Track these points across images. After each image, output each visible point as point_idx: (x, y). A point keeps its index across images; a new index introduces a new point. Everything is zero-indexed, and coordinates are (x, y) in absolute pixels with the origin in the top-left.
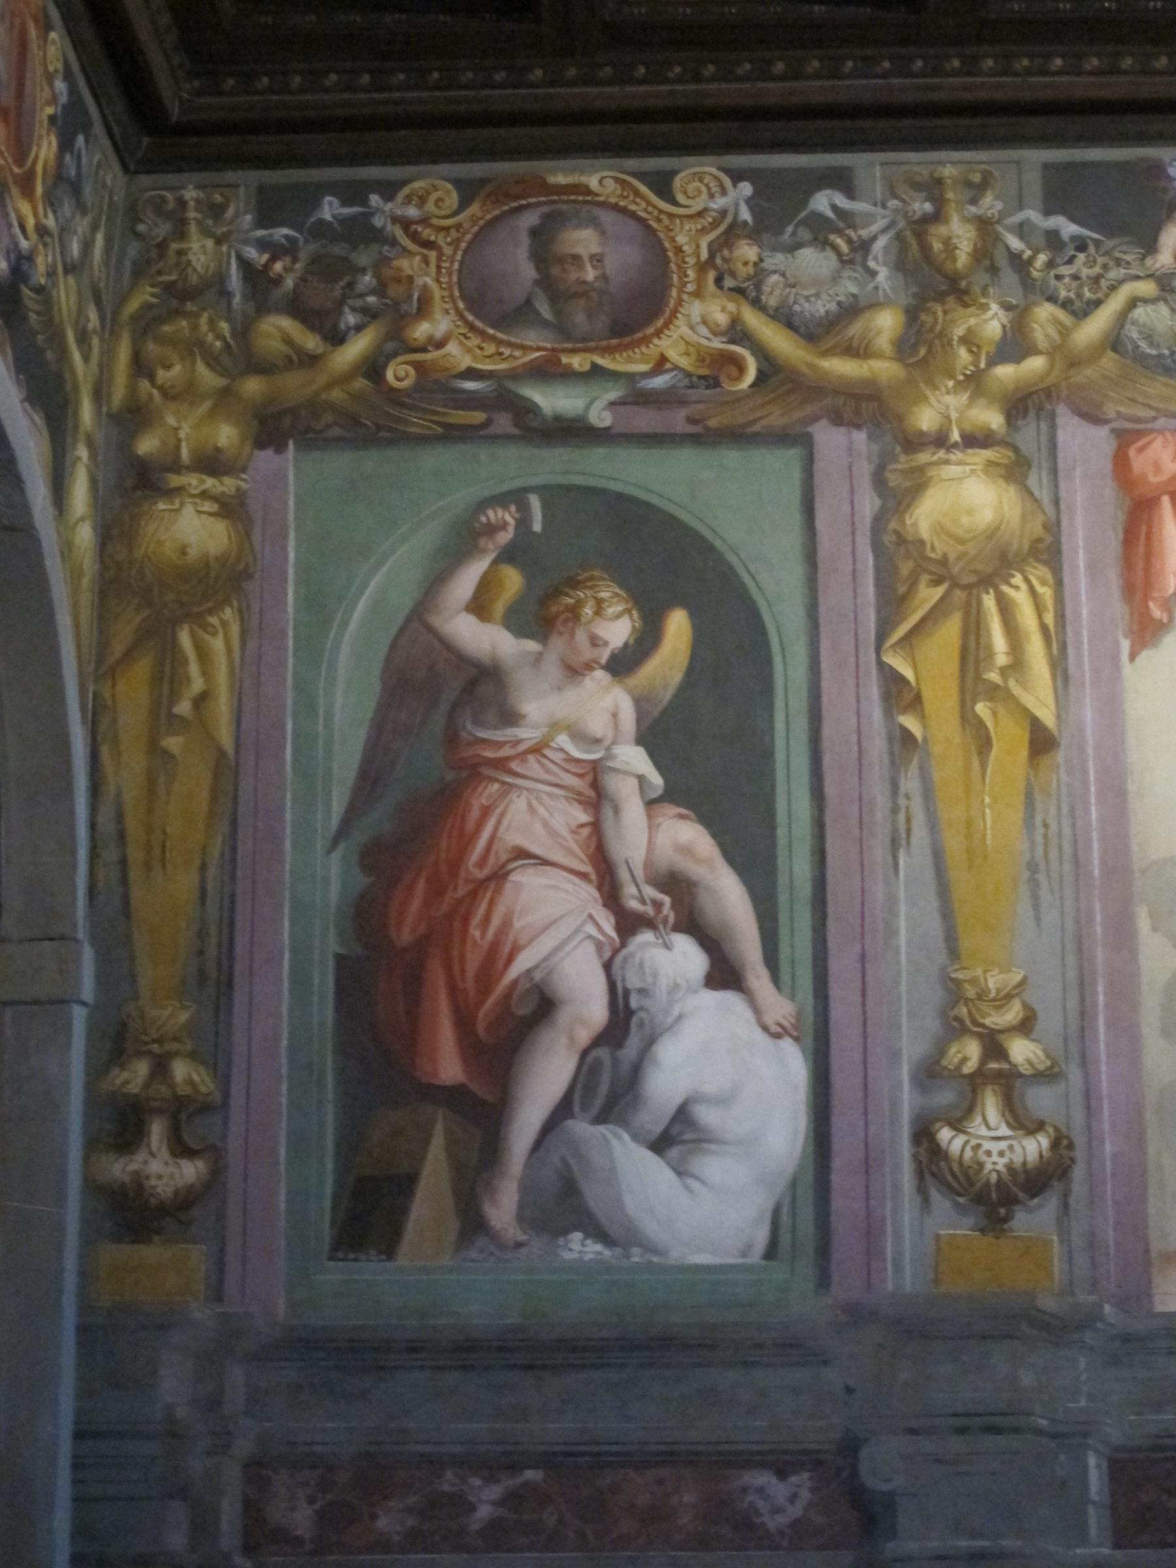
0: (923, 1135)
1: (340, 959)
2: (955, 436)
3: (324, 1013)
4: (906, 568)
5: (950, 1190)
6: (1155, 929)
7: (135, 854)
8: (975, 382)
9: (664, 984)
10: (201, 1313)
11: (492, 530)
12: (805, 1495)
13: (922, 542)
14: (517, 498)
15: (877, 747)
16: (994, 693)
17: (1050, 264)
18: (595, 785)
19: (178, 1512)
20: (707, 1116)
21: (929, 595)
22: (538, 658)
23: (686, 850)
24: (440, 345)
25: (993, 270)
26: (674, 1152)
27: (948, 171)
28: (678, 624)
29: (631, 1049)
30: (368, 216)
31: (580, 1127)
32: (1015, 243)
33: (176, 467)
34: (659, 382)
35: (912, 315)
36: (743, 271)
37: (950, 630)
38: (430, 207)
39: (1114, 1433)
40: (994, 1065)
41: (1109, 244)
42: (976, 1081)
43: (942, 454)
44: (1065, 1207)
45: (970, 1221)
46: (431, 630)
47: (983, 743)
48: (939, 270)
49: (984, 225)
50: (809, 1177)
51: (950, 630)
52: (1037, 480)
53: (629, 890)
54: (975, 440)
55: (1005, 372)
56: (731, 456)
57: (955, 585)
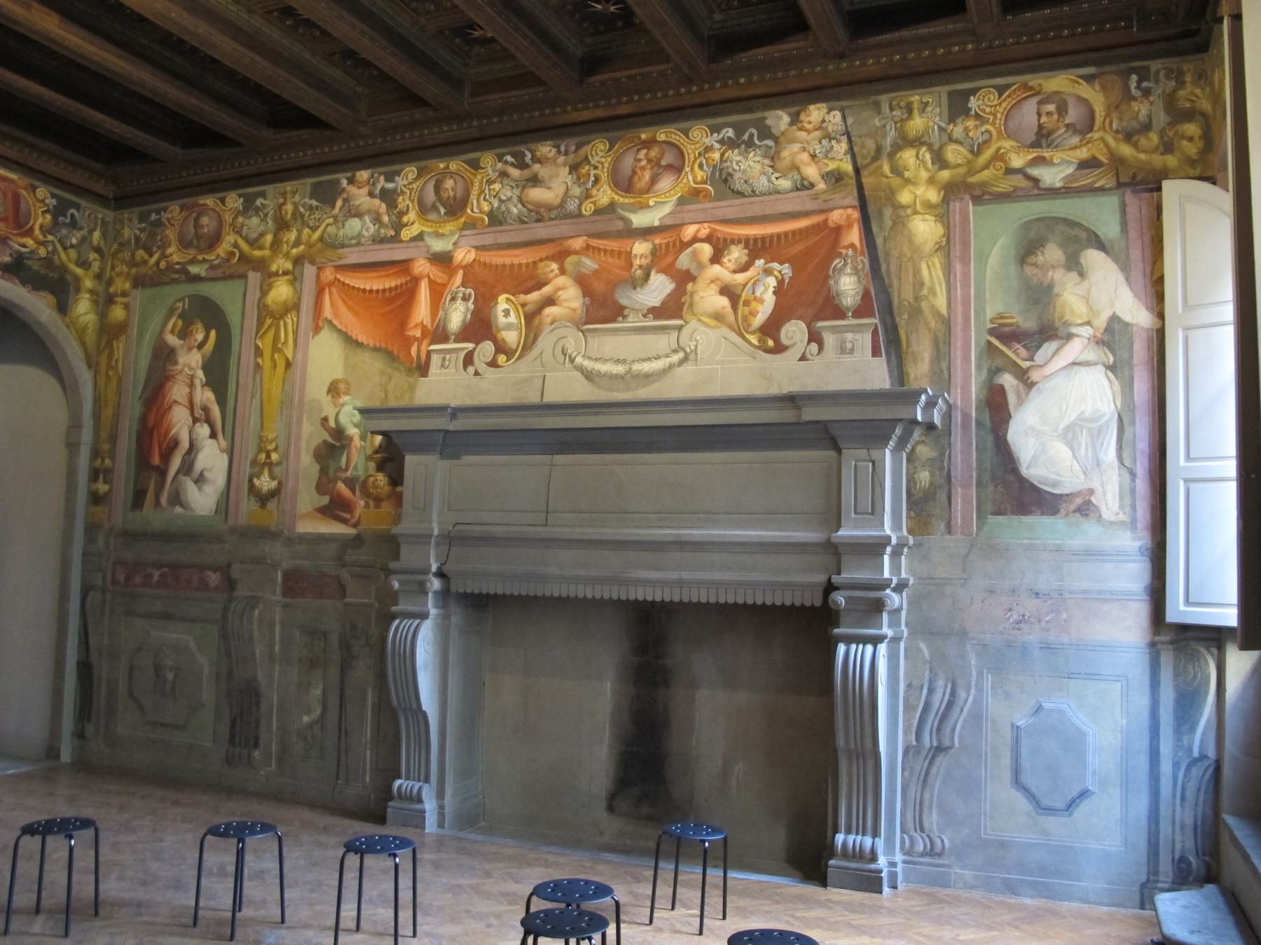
0: (250, 480)
1: (137, 431)
2: (281, 272)
3: (134, 447)
6: (307, 420)
7: (102, 404)
8: (287, 255)
9: (200, 439)
11: (178, 308)
12: (219, 578)
13: (268, 306)
14: (182, 299)
15: (251, 367)
16: (280, 351)
17: (309, 215)
19: (100, 574)
20: (207, 474)
21: (269, 321)
22: (183, 346)
23: (208, 399)
24: (171, 255)
25: (295, 219)
26: (199, 484)
27: (288, 188)
28: (213, 333)
30: (160, 218)
31: (181, 477)
32: (302, 209)
33: (116, 295)
34: (216, 262)
35: (275, 235)
36: (239, 225)
37: (272, 332)
38: (174, 214)
39: (285, 565)
40: (268, 461)
41: (324, 207)
42: (264, 464)
43: (277, 278)
44: (279, 501)
45: (258, 504)
47: (275, 366)
48: (283, 220)
49: (295, 205)
50: (225, 492)
53: (196, 411)
54: (285, 273)
55: (294, 251)
56: (229, 283)
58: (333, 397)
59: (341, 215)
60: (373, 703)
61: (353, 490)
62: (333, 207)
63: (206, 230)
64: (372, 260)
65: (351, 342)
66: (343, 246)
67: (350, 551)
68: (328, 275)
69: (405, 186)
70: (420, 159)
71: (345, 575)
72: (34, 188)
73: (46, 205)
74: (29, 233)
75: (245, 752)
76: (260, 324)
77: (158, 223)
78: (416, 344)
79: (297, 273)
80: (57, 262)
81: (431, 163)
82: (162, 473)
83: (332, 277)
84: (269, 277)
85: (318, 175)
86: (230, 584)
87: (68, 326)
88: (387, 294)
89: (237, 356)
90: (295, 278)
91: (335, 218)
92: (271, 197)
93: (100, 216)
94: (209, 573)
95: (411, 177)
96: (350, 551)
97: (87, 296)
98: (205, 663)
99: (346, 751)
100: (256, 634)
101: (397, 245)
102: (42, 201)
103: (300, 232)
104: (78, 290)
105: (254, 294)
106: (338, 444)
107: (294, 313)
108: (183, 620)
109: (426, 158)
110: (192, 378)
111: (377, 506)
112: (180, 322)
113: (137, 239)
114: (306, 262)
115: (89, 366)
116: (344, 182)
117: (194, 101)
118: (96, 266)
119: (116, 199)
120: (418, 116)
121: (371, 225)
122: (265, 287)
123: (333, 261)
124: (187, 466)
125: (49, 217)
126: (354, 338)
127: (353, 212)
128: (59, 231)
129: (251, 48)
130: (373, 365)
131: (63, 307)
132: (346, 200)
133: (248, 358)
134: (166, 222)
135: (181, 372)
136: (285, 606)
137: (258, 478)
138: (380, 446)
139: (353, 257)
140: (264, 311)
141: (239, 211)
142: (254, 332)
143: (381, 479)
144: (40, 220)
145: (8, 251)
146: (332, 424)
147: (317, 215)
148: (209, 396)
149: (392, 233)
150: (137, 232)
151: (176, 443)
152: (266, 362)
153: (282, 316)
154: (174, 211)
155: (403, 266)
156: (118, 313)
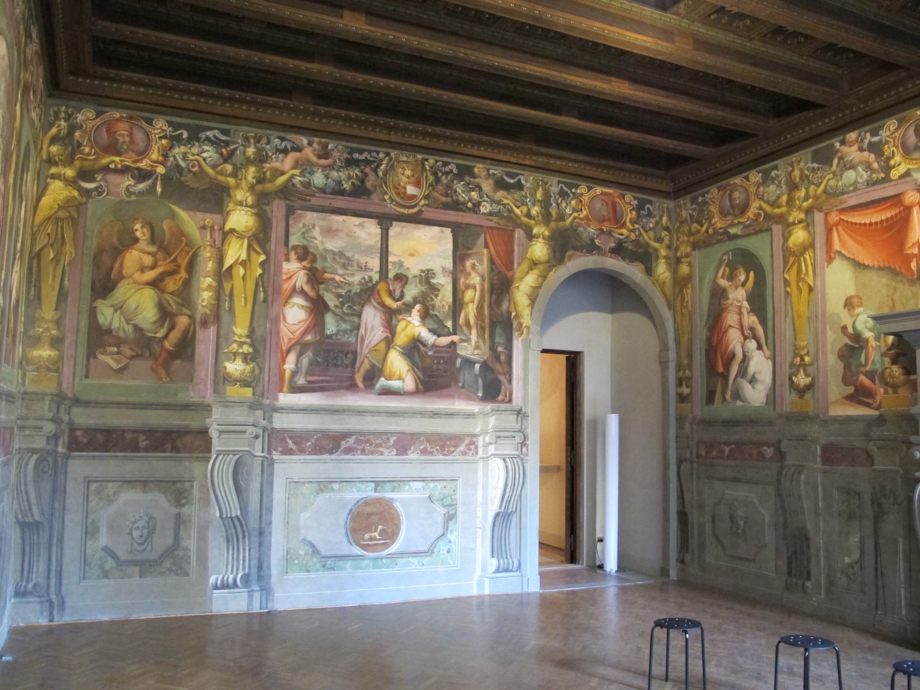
0: (790, 378)
1: (706, 350)
3: (704, 360)
4: (788, 255)
5: (794, 390)
6: (830, 329)
8: (800, 208)
10: (690, 415)
11: (725, 260)
14: (727, 253)
15: (783, 296)
16: (804, 280)
18: (740, 310)
19: (689, 451)
20: (757, 376)
21: (792, 259)
22: (731, 285)
23: (754, 322)
24: (716, 223)
25: (803, 180)
28: (752, 274)
29: (746, 364)
31: (739, 379)
32: (807, 172)
33: (682, 258)
34: (748, 222)
36: (761, 193)
37: (795, 268)
39: (823, 441)
42: (800, 366)
46: (716, 283)
47: (800, 292)
49: (801, 170)
51: (795, 268)
52: (811, 228)
54: (800, 222)
55: (805, 204)
56: (760, 236)
57: (796, 256)
58: (849, 310)
59: (838, 170)
60: (904, 552)
61: (873, 380)
62: (831, 166)
63: (738, 201)
64: (868, 200)
65: (858, 266)
66: (843, 193)
67: (874, 429)
68: (834, 217)
69: (888, 136)
70: (899, 112)
71: (872, 447)
72: (623, 196)
73: (632, 205)
74: (624, 225)
75: (800, 582)
76: (786, 261)
77: (705, 203)
78: (915, 260)
79: (809, 220)
80: (643, 241)
81: (908, 113)
82: (725, 377)
83: (837, 218)
84: (788, 227)
85: (816, 144)
86: (781, 456)
87: (653, 283)
88: (885, 224)
89: (771, 289)
90: (808, 224)
91: (834, 173)
92: (781, 168)
93: (665, 206)
94: (765, 448)
95: (892, 128)
96: (874, 429)
97: (663, 261)
98: (766, 515)
99: (883, 587)
100: (803, 493)
101: (887, 185)
102: (629, 203)
103: (807, 189)
104: (657, 258)
105: (778, 242)
106: (857, 346)
107: (811, 250)
108: (748, 482)
109: (904, 110)
110: (740, 308)
111: (895, 392)
112: (727, 270)
113: (691, 216)
114: (815, 211)
115: (670, 308)
116: (837, 145)
117: (719, 113)
118: (667, 239)
119: (674, 192)
120: (892, 79)
121: (864, 173)
122: (786, 235)
123: (836, 206)
124: (743, 372)
125: (634, 213)
126: (861, 261)
127: (848, 166)
128: (642, 221)
129: (755, 65)
130: (879, 282)
131: (649, 271)
132: (841, 158)
133: (779, 288)
134: (709, 201)
135: (732, 304)
136: (825, 472)
137: (796, 376)
138: (893, 344)
139: (852, 200)
140: (787, 252)
141: (760, 183)
142: (782, 269)
143: (896, 370)
144: (629, 216)
145: (613, 240)
146: (850, 330)
147: (819, 175)
148: (751, 320)
149: (883, 175)
150: (691, 212)
151: (733, 355)
152: (793, 289)
153: (802, 254)
154: (714, 192)
155: (896, 199)
156: (684, 269)
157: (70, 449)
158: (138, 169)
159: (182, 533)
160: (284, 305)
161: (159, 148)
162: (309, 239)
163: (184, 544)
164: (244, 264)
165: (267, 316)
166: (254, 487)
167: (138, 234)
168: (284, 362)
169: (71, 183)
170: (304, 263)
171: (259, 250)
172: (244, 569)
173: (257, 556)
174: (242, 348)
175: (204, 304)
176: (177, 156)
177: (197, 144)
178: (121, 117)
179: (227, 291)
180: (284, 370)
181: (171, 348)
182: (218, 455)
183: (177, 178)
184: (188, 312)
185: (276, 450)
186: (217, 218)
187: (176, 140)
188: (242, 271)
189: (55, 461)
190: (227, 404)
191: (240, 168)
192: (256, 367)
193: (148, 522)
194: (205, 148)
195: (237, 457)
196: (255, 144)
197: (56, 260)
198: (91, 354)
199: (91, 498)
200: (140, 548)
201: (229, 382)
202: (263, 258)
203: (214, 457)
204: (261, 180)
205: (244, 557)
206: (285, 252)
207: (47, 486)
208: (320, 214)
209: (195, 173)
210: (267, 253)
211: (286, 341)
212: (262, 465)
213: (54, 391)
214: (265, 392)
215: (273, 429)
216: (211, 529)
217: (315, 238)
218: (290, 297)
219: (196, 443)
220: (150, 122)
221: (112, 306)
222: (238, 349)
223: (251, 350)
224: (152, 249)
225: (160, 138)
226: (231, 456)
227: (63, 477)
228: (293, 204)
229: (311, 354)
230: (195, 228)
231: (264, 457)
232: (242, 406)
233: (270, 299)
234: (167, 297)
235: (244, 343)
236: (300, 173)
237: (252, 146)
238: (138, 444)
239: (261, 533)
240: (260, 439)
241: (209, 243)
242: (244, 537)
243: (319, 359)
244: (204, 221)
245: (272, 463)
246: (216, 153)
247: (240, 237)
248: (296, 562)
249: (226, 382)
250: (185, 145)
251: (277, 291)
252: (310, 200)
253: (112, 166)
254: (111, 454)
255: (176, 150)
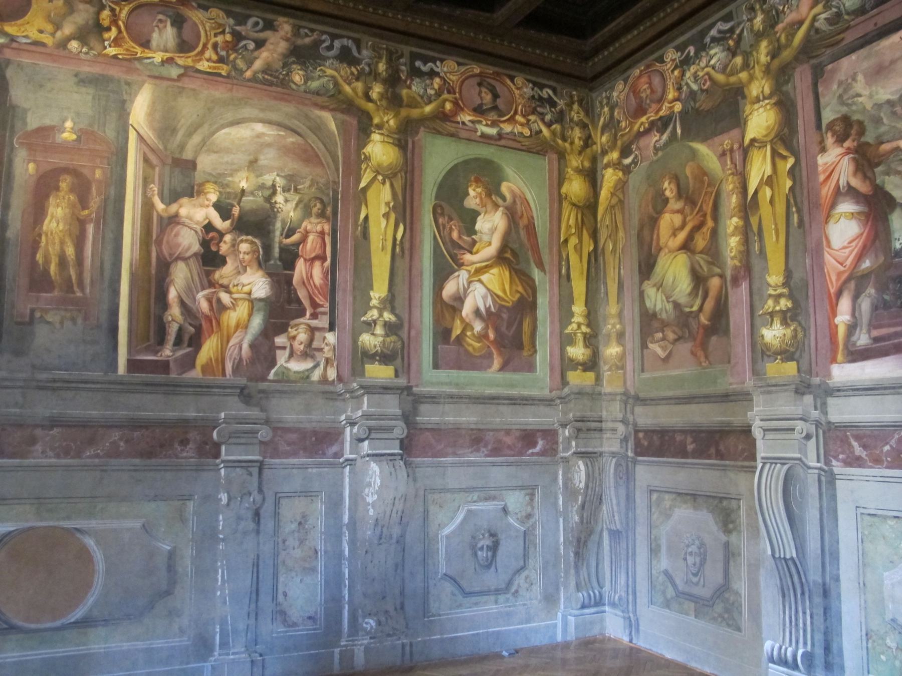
157: (637, 454)
158: (661, 118)
159: (732, 570)
160: (827, 222)
161: (673, 84)
162: (850, 101)
163: (735, 586)
164: (769, 182)
165: (806, 248)
166: (811, 516)
167: (668, 193)
168: (834, 314)
169: (617, 165)
170: (848, 144)
171: (785, 153)
172: (805, 643)
173: (822, 627)
174: (779, 303)
175: (733, 254)
176: (689, 81)
177: (704, 54)
178: (641, 71)
179: (755, 228)
180: (837, 326)
181: (706, 322)
182: (764, 464)
183: (692, 108)
184: (718, 270)
185: (836, 458)
186: (735, 133)
187: (686, 62)
188: (768, 192)
189: (627, 465)
190: (771, 388)
191: (751, 53)
192: (799, 329)
193: (699, 548)
194: (712, 52)
195: (786, 467)
196: (761, 7)
197: (614, 250)
198: (644, 346)
199: (653, 510)
200: (695, 580)
201: (769, 356)
202: (791, 161)
203: (760, 466)
204: (774, 55)
205: (805, 624)
206: (819, 139)
207: (622, 492)
208: (863, 52)
209: (707, 90)
210: (795, 153)
211: (834, 278)
212: (820, 481)
213: (621, 390)
214: (814, 365)
215: (829, 422)
216: (762, 571)
217: (859, 95)
218: (833, 205)
219: (740, 447)
220: (661, 60)
221: (655, 285)
222: (775, 307)
223: (789, 304)
224: (678, 205)
225: (673, 71)
226: (779, 465)
227: (633, 483)
228: (822, 59)
229: (873, 291)
230: (715, 159)
231: (820, 469)
232: (786, 391)
233: (806, 219)
234: (697, 258)
235: (780, 296)
236: (824, 7)
237: (759, 13)
238: (686, 447)
239: (826, 593)
240: (814, 440)
241: (730, 172)
242: (803, 593)
243: (887, 297)
244: (722, 145)
245: (832, 479)
246: (723, 51)
247: (763, 145)
248: (883, 657)
249: (765, 357)
250: (694, 63)
251: (815, 204)
252: (843, 39)
253: (642, 129)
254: (665, 459)
255: (688, 74)
